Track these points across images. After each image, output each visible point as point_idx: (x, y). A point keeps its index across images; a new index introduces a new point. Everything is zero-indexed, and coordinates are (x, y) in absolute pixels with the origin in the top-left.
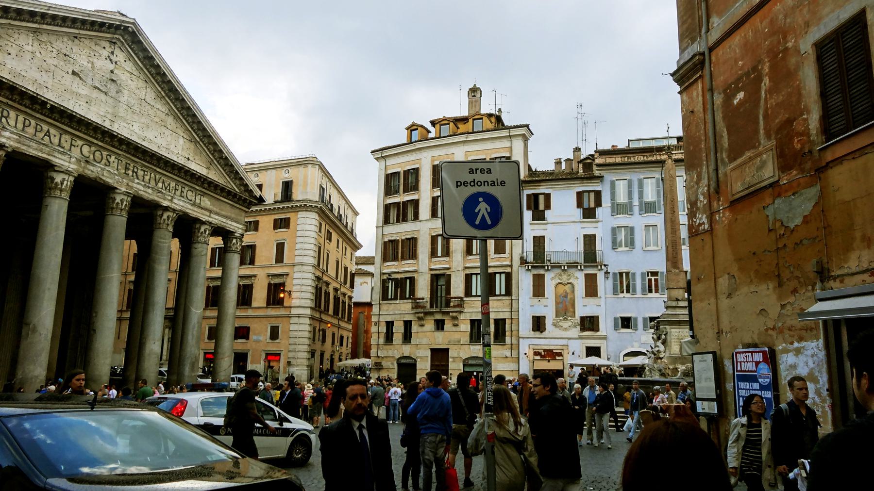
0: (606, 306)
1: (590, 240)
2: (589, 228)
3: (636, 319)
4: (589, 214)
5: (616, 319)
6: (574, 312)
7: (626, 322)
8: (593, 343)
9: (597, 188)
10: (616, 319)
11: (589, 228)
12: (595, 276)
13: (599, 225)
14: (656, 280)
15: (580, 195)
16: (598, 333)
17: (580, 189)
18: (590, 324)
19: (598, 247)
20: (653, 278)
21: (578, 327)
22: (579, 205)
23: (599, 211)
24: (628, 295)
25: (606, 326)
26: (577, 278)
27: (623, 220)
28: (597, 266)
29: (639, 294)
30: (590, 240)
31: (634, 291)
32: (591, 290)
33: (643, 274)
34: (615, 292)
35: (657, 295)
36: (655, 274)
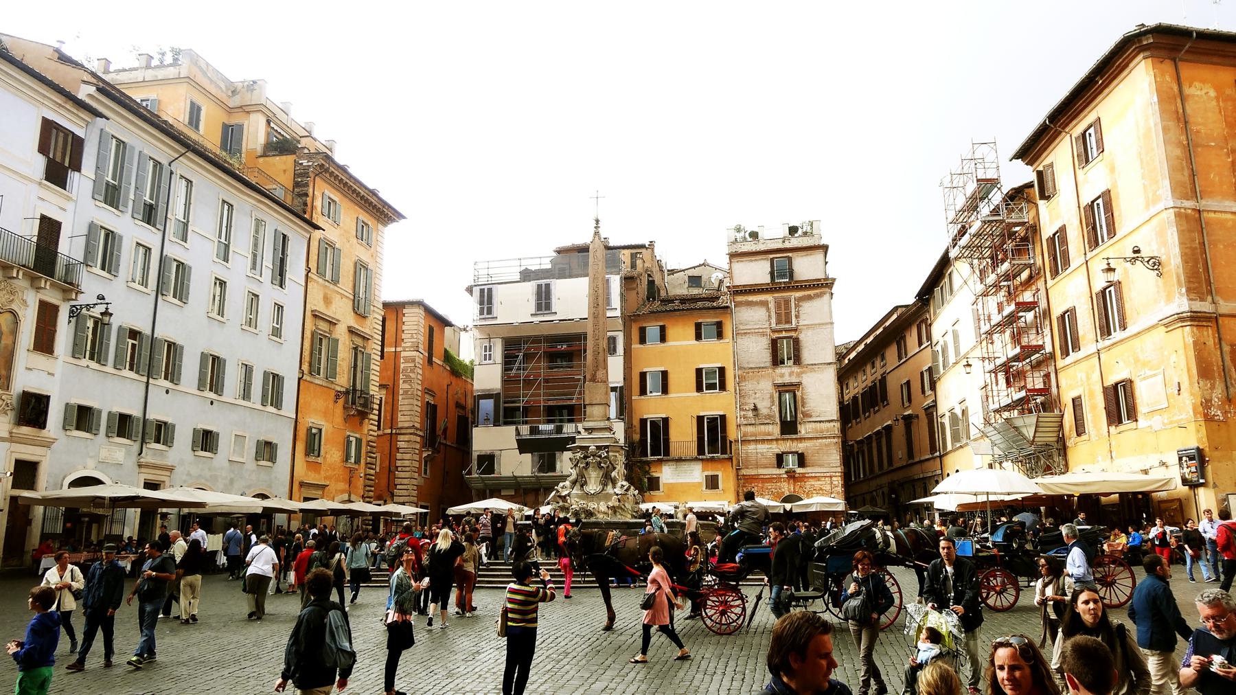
0: (58, 377)
1: (50, 229)
2: (52, 203)
3: (100, 412)
4: (57, 175)
6: (8, 378)
7: (83, 417)
8: (28, 453)
9: (80, 132)
11: (52, 203)
12: (55, 309)
13: (70, 206)
15: (48, 127)
16: (44, 433)
17: (52, 116)
18: (32, 410)
19: (64, 247)
20: (131, 341)
21: (11, 416)
22: (43, 149)
23: (73, 177)
24: (93, 365)
26: (25, 302)
27: (108, 218)
28: (72, 290)
29: (109, 368)
30: (50, 229)
31: (106, 360)
32: (44, 343)
35: (132, 375)
36: (134, 334)
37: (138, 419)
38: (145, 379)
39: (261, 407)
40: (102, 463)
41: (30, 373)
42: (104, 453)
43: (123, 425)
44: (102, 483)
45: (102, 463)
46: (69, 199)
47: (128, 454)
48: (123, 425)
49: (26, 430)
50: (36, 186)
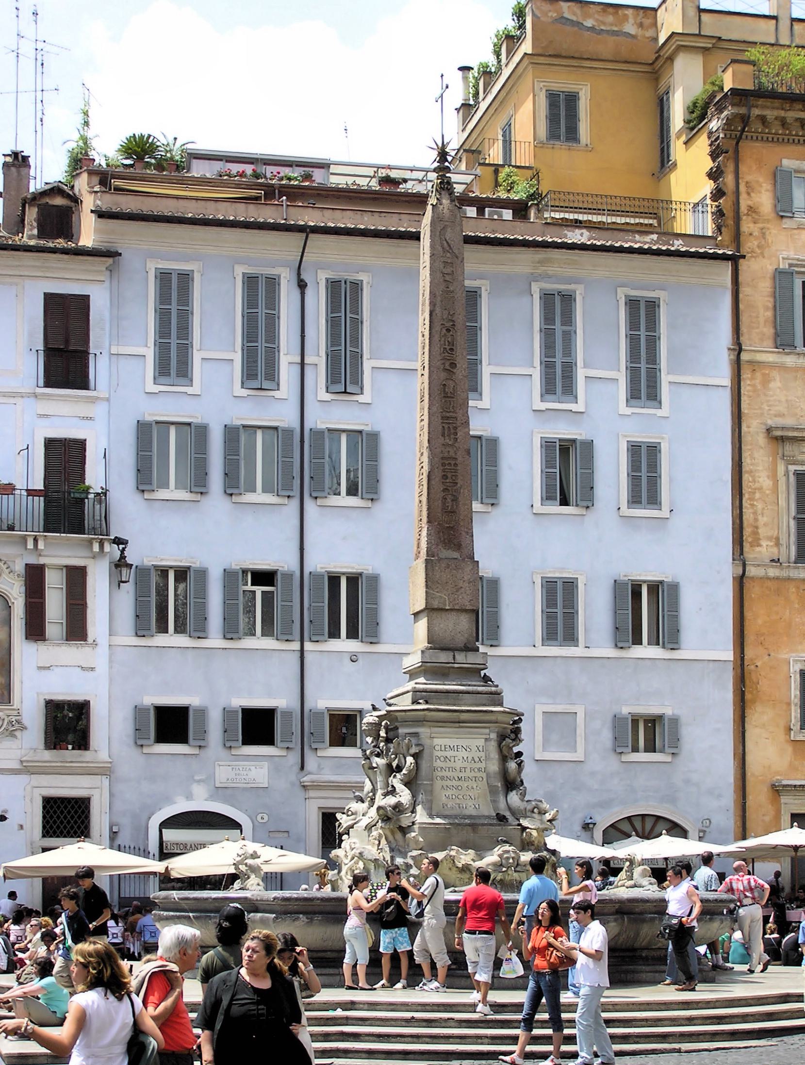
1: (65, 456)
2: (65, 415)
3: (202, 712)
5: (139, 711)
7: (172, 724)
8: (67, 787)
10: (139, 711)
13: (99, 411)
14: (268, 599)
20: (259, 590)
25: (109, 728)
29: (215, 641)
33: (229, 576)
34: (141, 630)
35: (269, 643)
36: (263, 577)
37: (288, 714)
38: (296, 646)
39: (612, 653)
40: (220, 792)
41: (43, 673)
42: (224, 774)
43: (258, 726)
44: (234, 825)
45: (220, 792)
46: (94, 400)
47: (276, 771)
48: (258, 726)
49: (70, 754)
50: (32, 400)
